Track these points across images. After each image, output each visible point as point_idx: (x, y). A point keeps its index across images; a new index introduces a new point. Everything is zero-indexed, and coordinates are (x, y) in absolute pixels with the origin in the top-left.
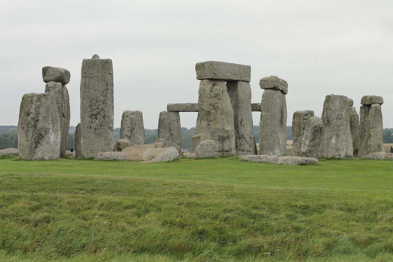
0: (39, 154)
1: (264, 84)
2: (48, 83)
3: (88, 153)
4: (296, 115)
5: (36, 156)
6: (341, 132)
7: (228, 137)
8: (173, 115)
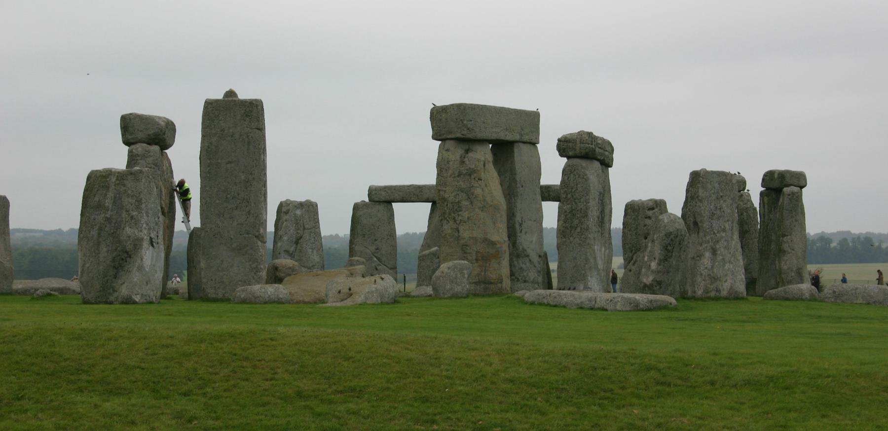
1: (565, 146)
2: (133, 146)
4: (632, 209)
6: (720, 246)
7: (497, 255)
8: (381, 207)
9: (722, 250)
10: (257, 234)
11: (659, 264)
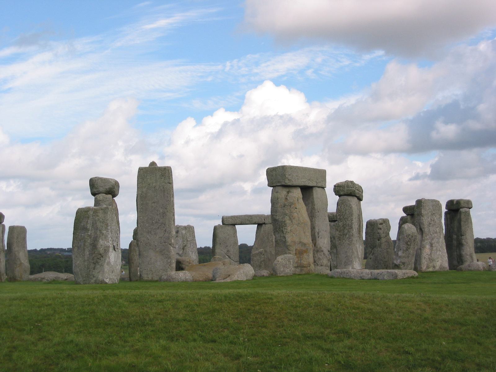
3: (147, 274)
7: (306, 251)
8: (230, 228)
9: (436, 243)
10: (170, 243)
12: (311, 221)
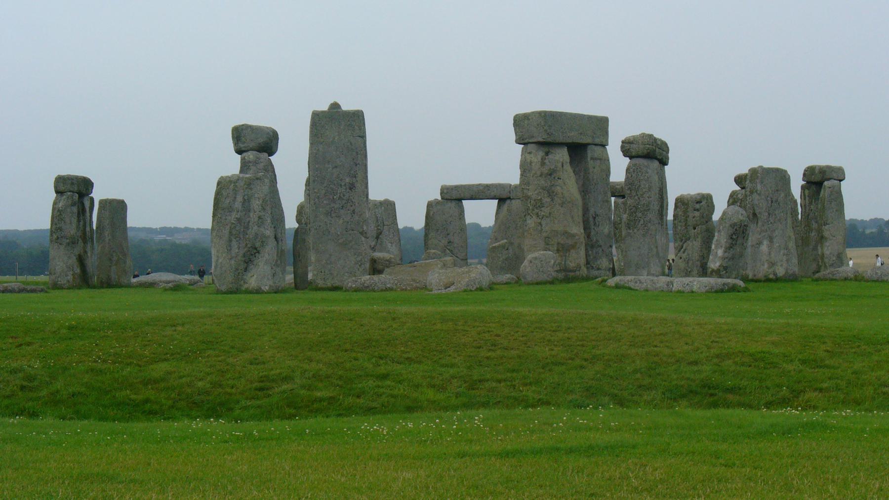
0: (252, 281)
1: (627, 148)
2: (244, 154)
4: (681, 202)
5: (246, 286)
7: (573, 247)
8: (453, 205)
11: (725, 252)
12: (584, 199)
